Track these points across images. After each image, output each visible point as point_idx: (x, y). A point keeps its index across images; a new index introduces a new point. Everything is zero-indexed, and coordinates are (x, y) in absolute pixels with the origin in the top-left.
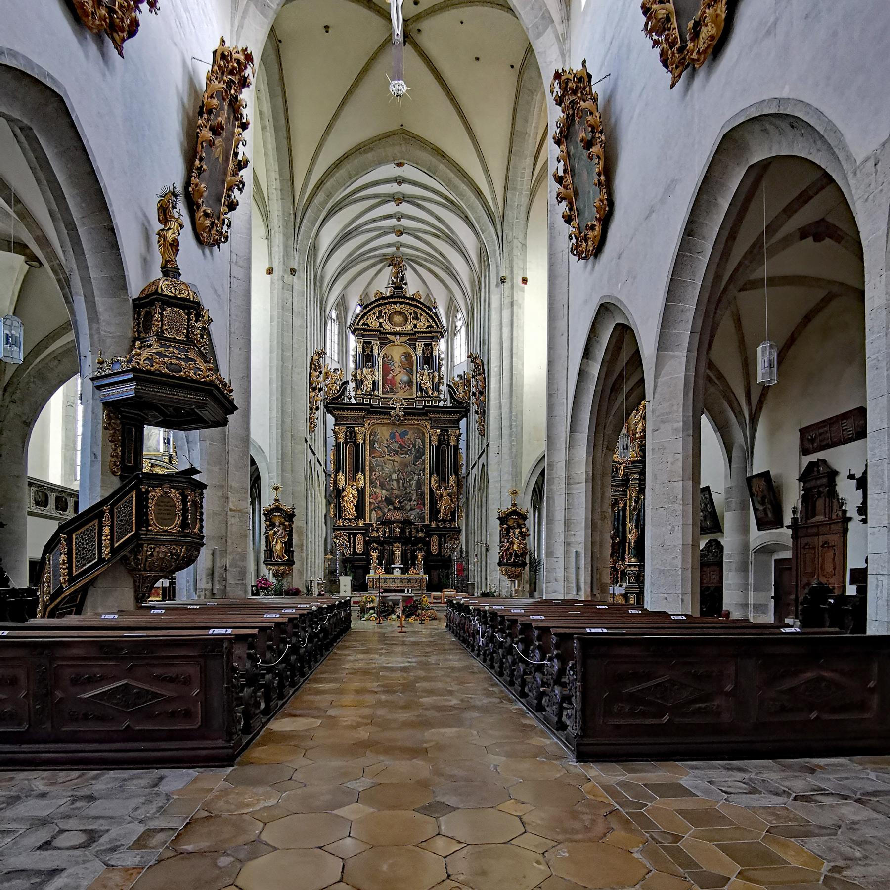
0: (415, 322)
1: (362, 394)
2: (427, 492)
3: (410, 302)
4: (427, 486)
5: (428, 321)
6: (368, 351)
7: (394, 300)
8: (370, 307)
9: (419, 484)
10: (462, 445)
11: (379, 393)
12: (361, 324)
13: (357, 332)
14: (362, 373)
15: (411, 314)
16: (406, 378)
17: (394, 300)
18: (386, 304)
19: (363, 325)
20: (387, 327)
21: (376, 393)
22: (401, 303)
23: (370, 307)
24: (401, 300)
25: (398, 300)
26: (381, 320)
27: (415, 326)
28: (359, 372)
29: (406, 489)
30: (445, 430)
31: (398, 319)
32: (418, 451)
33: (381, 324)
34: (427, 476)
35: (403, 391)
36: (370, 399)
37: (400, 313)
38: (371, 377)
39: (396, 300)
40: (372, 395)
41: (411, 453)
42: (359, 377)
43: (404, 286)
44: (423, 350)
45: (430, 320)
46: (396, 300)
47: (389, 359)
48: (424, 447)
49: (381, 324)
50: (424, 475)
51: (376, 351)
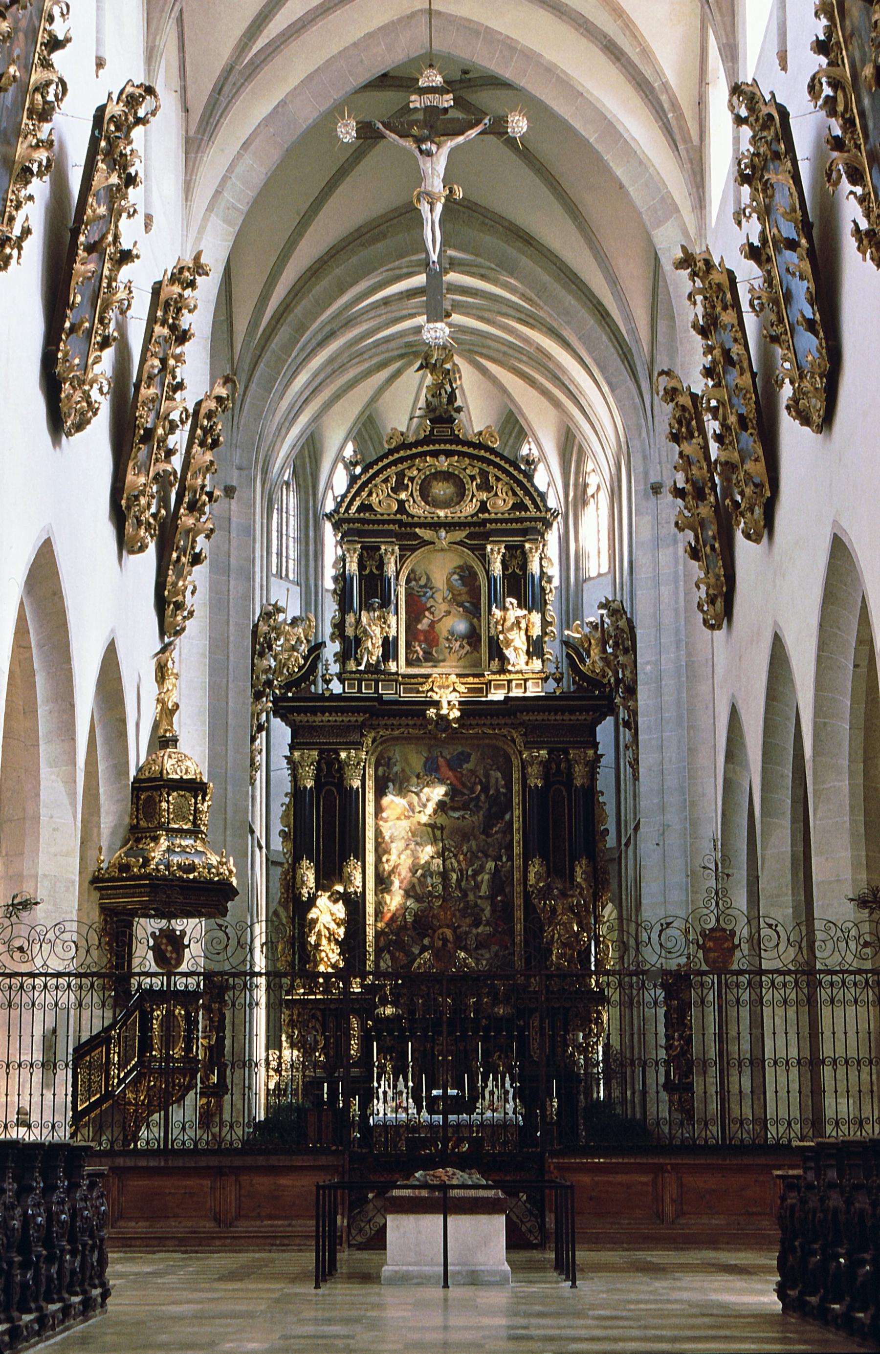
0: (484, 496)
1: (358, 672)
2: (519, 901)
3: (471, 450)
4: (518, 889)
5: (515, 494)
6: (371, 567)
7: (431, 447)
8: (376, 468)
9: (500, 882)
10: (605, 781)
11: (399, 666)
12: (354, 509)
13: (345, 527)
14: (358, 621)
15: (473, 478)
16: (461, 627)
17: (431, 447)
18: (413, 457)
19: (359, 510)
20: (418, 509)
21: (392, 667)
22: (449, 454)
23: (376, 468)
24: (448, 447)
25: (443, 447)
26: (403, 496)
27: (483, 507)
28: (350, 619)
29: (465, 895)
30: (558, 750)
31: (441, 489)
32: (493, 800)
33: (401, 503)
34: (518, 862)
35: (455, 657)
36: (377, 682)
37: (446, 476)
38: (378, 630)
39: (437, 447)
40: (383, 672)
41: (476, 806)
42: (350, 632)
43: (455, 415)
44: (503, 562)
45: (518, 490)
46: (437, 447)
47: (423, 582)
48: (510, 790)
49: (401, 503)
50: (510, 858)
51: (391, 569)
